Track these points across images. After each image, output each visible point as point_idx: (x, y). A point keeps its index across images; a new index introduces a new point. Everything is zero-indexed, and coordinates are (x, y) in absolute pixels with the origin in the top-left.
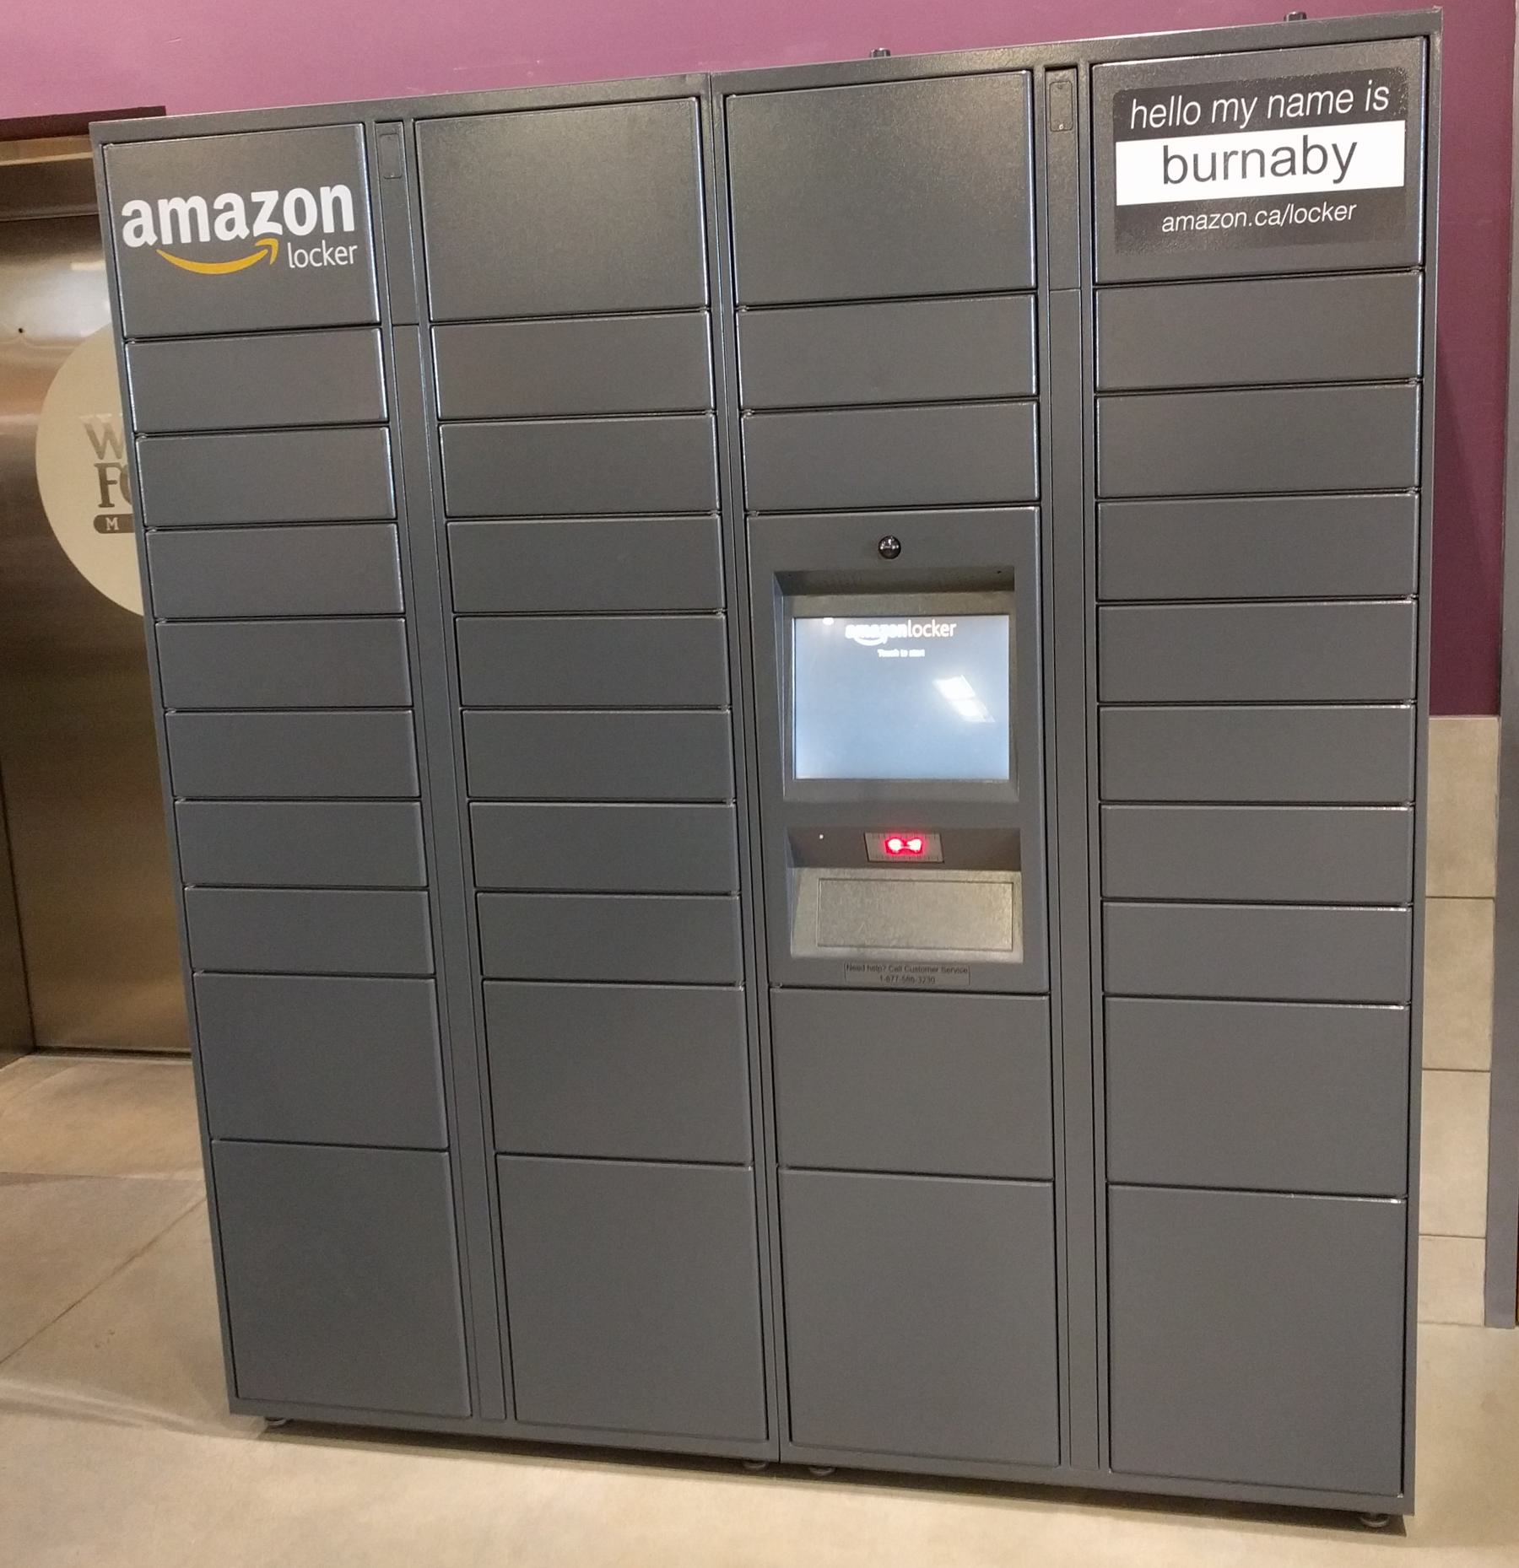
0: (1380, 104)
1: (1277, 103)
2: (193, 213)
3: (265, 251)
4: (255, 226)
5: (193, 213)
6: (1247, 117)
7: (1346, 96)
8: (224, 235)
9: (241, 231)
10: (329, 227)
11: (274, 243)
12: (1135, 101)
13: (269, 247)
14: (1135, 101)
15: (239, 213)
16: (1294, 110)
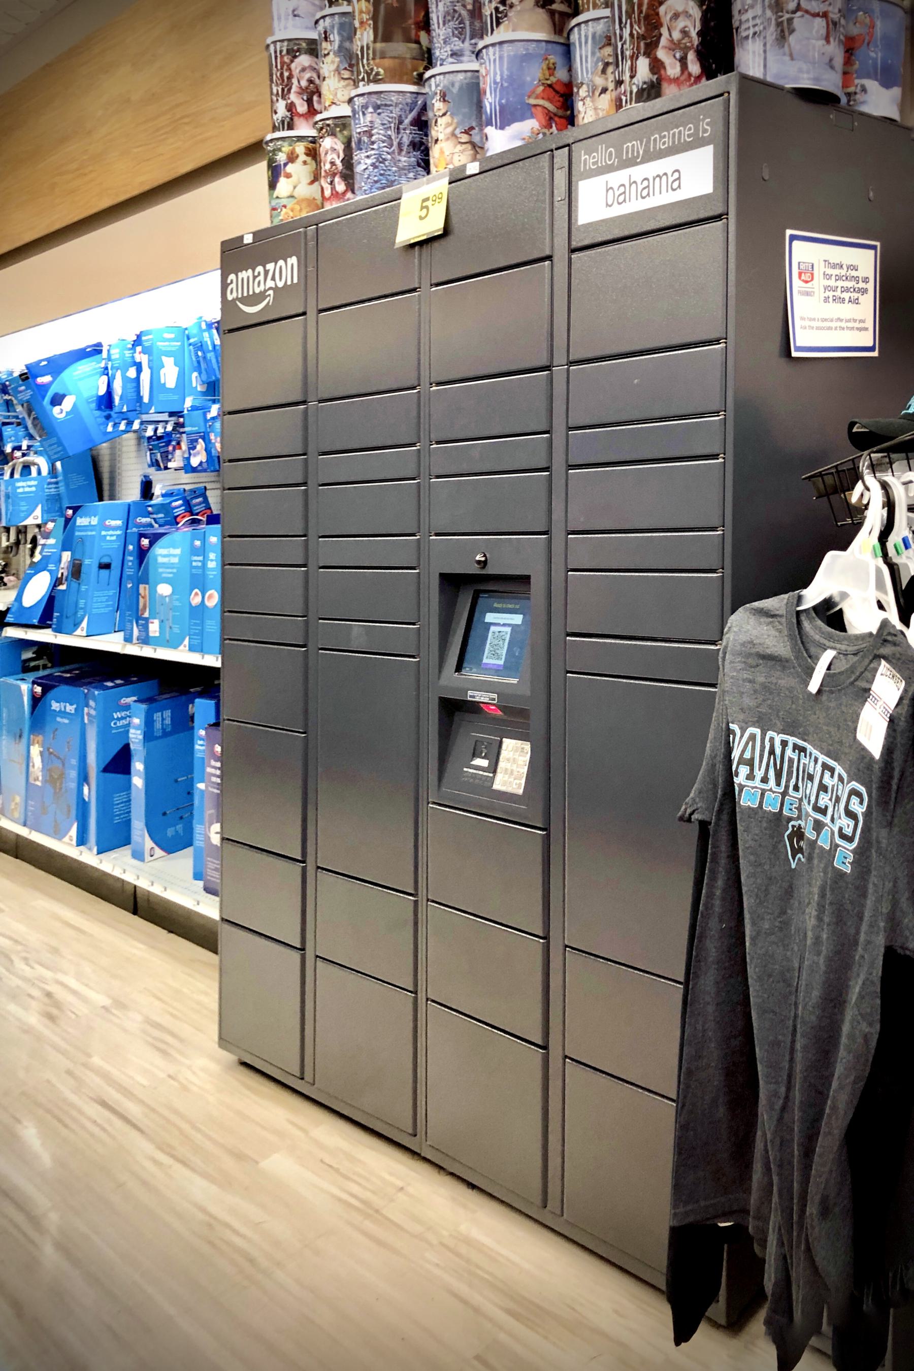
0: (705, 131)
1: (655, 140)
2: (248, 278)
3: (268, 298)
4: (267, 284)
5: (248, 278)
6: (641, 152)
7: (690, 129)
8: (257, 291)
9: (262, 288)
10: (289, 283)
11: (271, 292)
12: (583, 152)
13: (269, 295)
14: (583, 152)
15: (261, 278)
16: (664, 143)
